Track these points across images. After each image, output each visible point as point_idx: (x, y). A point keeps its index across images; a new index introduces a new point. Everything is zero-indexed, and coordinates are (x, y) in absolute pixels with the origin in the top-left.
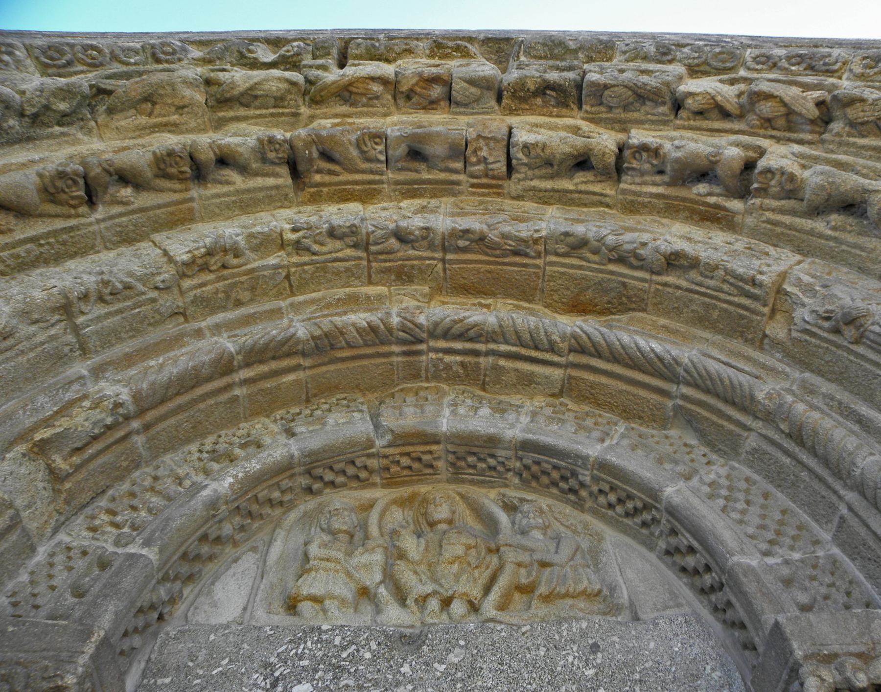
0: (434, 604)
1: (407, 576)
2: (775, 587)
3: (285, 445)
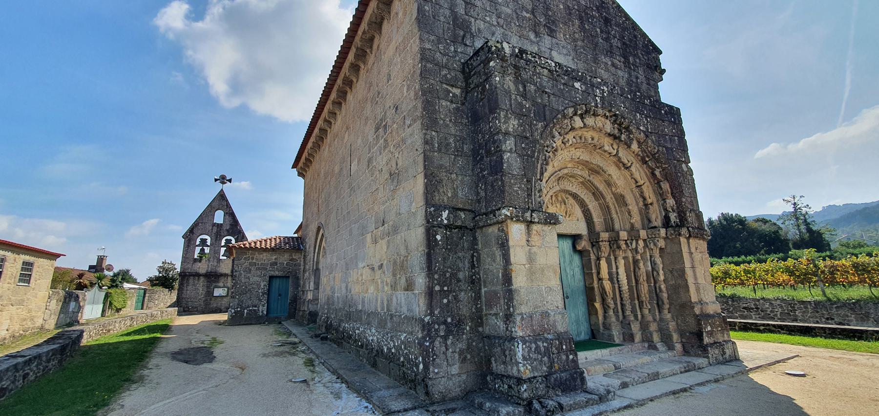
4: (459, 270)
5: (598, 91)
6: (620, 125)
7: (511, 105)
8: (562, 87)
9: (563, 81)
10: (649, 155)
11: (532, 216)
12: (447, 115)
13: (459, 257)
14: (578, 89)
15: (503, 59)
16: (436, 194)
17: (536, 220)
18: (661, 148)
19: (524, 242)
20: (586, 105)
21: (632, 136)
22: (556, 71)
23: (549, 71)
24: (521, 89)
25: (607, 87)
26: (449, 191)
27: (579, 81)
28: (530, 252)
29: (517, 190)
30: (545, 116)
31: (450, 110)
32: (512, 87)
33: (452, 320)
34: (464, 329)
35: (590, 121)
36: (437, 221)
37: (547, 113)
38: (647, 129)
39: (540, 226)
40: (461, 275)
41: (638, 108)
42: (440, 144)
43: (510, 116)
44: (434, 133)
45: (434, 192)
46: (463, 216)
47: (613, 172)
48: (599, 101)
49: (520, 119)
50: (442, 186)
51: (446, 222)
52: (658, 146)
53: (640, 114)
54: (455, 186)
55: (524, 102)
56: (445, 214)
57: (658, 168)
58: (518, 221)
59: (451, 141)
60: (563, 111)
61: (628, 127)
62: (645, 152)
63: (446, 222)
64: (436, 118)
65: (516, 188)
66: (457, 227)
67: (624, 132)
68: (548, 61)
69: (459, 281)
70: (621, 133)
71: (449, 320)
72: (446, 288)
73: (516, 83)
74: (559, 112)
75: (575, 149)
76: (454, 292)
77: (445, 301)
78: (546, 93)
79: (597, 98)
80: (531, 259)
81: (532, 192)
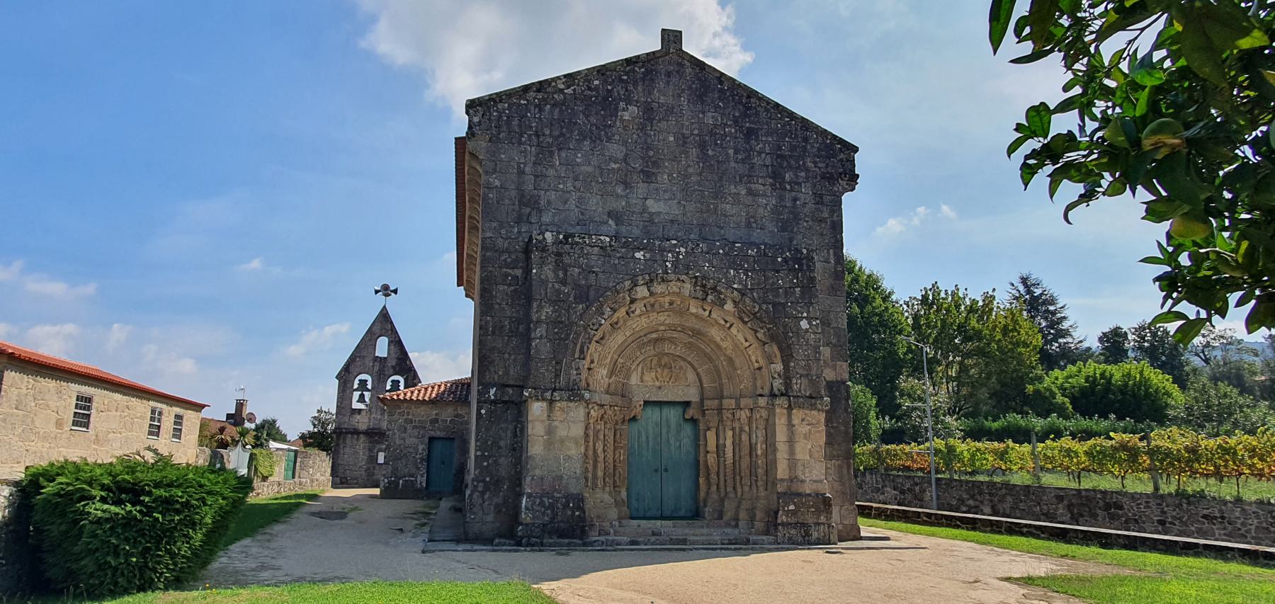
1: (659, 376)
4: (501, 439)
5: (670, 255)
6: (704, 286)
8: (616, 262)
9: (618, 255)
11: (552, 394)
12: (503, 298)
13: (502, 428)
14: (640, 259)
15: (544, 249)
16: (487, 373)
17: (558, 398)
18: (764, 307)
20: (649, 274)
21: (722, 296)
22: (611, 246)
23: (601, 248)
24: (561, 275)
25: (686, 248)
27: (642, 250)
28: (550, 425)
30: (588, 296)
32: (551, 275)
35: (659, 288)
37: (592, 293)
38: (746, 286)
39: (564, 403)
40: (502, 443)
41: (734, 262)
42: (494, 327)
43: (544, 304)
44: (489, 318)
46: (511, 392)
47: (715, 333)
48: (670, 266)
51: (493, 397)
52: (760, 305)
53: (735, 270)
55: (562, 288)
56: (492, 391)
57: (762, 328)
58: (538, 400)
59: (506, 323)
60: (615, 286)
61: (716, 287)
62: (744, 312)
63: (493, 397)
65: (544, 373)
66: (503, 402)
68: (602, 238)
69: (500, 448)
70: (708, 295)
71: (488, 479)
72: (486, 454)
73: (555, 271)
74: (607, 289)
76: (495, 456)
77: (485, 464)
78: (594, 272)
79: (667, 263)
80: (550, 431)
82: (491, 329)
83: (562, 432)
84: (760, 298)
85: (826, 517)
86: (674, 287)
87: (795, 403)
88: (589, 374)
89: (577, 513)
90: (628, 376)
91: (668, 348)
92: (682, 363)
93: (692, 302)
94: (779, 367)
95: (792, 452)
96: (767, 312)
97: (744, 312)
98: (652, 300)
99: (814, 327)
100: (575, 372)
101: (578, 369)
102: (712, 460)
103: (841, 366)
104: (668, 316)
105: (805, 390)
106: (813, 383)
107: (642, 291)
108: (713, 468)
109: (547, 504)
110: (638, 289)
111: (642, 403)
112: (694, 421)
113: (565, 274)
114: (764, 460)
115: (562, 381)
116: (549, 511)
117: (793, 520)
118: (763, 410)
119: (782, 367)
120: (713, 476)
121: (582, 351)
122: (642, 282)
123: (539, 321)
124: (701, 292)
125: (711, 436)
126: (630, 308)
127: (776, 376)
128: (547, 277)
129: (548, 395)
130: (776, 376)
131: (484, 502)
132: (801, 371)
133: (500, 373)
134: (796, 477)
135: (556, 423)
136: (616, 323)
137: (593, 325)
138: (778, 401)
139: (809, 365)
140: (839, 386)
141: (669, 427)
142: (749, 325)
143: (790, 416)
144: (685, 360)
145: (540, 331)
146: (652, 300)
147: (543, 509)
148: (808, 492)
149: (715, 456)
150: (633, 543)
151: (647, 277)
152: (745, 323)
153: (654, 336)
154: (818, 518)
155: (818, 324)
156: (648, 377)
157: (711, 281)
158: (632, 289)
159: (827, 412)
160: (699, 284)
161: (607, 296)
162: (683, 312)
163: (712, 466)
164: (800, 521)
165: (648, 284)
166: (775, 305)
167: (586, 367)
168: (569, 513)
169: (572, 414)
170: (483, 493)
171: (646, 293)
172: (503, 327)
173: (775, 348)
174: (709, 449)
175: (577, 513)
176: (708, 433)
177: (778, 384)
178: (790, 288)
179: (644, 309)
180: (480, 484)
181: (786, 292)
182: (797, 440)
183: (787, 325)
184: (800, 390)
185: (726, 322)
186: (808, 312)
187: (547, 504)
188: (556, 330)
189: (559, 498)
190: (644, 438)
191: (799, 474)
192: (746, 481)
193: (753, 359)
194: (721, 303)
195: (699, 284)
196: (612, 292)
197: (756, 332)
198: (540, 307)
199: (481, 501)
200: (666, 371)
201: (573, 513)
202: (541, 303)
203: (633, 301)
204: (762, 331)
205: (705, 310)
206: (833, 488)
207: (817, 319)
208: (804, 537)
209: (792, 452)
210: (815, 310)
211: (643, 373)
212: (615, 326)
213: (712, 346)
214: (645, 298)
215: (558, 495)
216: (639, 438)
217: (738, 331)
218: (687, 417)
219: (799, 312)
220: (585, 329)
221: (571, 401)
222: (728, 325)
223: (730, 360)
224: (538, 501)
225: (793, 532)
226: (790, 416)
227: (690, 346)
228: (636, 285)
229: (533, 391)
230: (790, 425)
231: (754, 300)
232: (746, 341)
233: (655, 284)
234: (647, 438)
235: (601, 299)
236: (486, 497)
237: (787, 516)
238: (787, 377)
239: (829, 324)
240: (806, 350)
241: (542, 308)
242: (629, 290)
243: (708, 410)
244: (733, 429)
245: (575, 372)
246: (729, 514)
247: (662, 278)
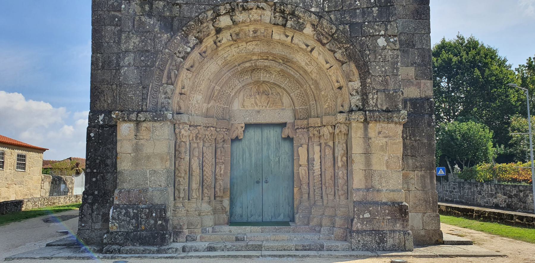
0: (261, 107)
1: (257, 102)
2: (299, 112)
3: (239, 85)
4: (108, 158)
6: (283, 12)
7: (134, 26)
10: (327, 36)
11: (137, 116)
13: (108, 148)
16: (98, 102)
18: (341, 27)
19: (132, 136)
20: (230, 4)
21: (301, 21)
24: (147, 8)
26: (109, 98)
28: (137, 144)
29: (132, 96)
31: (114, 33)
32: (138, 9)
33: (99, 193)
34: (108, 200)
35: (240, 17)
36: (94, 122)
37: (176, 23)
38: (323, 9)
39: (149, 124)
42: (103, 63)
43: (131, 35)
44: (99, 55)
45: (96, 101)
47: (300, 59)
49: (142, 36)
50: (103, 96)
51: (101, 123)
54: (114, 94)
56: (101, 117)
57: (340, 48)
59: (114, 58)
60: (198, 16)
62: (322, 35)
63: (101, 123)
64: (102, 43)
67: (290, 18)
69: (107, 165)
70: (287, 21)
71: (96, 193)
72: (95, 171)
73: (142, 6)
74: (190, 19)
75: (247, 43)
77: (94, 179)
78: (177, 4)
80: (137, 149)
81: (147, 96)
82: (100, 64)
83: (148, 149)
84: (337, 19)
85: (403, 224)
86: (255, 15)
87: (371, 117)
88: (180, 98)
89: (160, 222)
90: (231, 103)
91: (263, 76)
92: (279, 90)
93: (275, 29)
94: (357, 84)
95: (368, 163)
96: (343, 32)
97: (322, 35)
98: (237, 29)
99: (391, 44)
100: (163, 96)
101: (166, 93)
102: (303, 172)
103: (425, 84)
104: (256, 45)
105: (381, 105)
106: (390, 97)
107: (225, 21)
108: (305, 181)
109: (132, 214)
110: (221, 18)
111: (243, 125)
112: (289, 139)
113: (151, 8)
114: (345, 172)
115: (149, 104)
116: (134, 221)
117: (368, 227)
118: (343, 125)
119: (360, 84)
120: (305, 186)
121: (169, 77)
122: (224, 12)
123: (127, 51)
124: (281, 19)
125: (302, 152)
126: (217, 38)
127: (354, 93)
128: (134, 11)
129: (133, 116)
130: (354, 93)
131: (93, 212)
132: (378, 87)
133: (109, 102)
134: (372, 187)
135: (142, 142)
136: (205, 52)
137: (180, 53)
138: (354, 116)
139: (386, 81)
140: (423, 102)
141: (269, 144)
142: (327, 46)
143: (366, 129)
144: (280, 86)
145: (129, 59)
146: (237, 29)
147: (128, 219)
148: (384, 201)
149: (306, 169)
150: (211, 249)
151: (228, 6)
152: (324, 45)
153: (248, 65)
154: (394, 225)
155: (396, 41)
156: (249, 102)
157: (289, 6)
158: (215, 18)
159: (405, 126)
160: (278, 10)
161: (190, 26)
162: (268, 40)
163: (303, 177)
164: (376, 228)
165: (231, 12)
166: (351, 25)
167: (177, 91)
168: (152, 222)
169: (157, 133)
170: (92, 204)
171: (231, 23)
172: (110, 62)
173: (353, 66)
174: (301, 163)
175: (160, 222)
176: (300, 148)
177: (356, 100)
178: (368, 8)
179: (230, 38)
180: (90, 197)
181: (363, 13)
182: (373, 152)
183: (364, 43)
184: (376, 105)
185: (307, 46)
186: (386, 30)
187: (132, 214)
188: (143, 58)
189: (143, 209)
190: (247, 155)
191: (376, 184)
192: (330, 191)
193: (334, 78)
194: (300, 28)
195: (278, 10)
196: (195, 22)
197: (334, 52)
198: (128, 38)
199: (90, 211)
200: (264, 97)
201: (156, 222)
202: (129, 34)
203: (218, 31)
204: (340, 51)
205: (287, 36)
206: (416, 197)
207: (395, 36)
208: (379, 244)
209: (368, 163)
210: (393, 28)
211: (244, 100)
212: (203, 54)
213: (301, 72)
214: (229, 28)
215: (143, 206)
216: (243, 155)
217: (319, 54)
218: (283, 136)
219: (376, 31)
220: (171, 56)
221: (155, 121)
222: (309, 49)
223: (316, 84)
224: (124, 211)
225: (368, 239)
226: (366, 129)
227: (283, 74)
228: (219, 15)
229: (120, 113)
230: (367, 138)
231: (331, 21)
232: (327, 63)
233: (237, 13)
234: (250, 155)
235: (184, 29)
236: (95, 207)
237: (362, 224)
238: (364, 95)
239: (414, 45)
240: (383, 67)
241: (130, 39)
242: (212, 20)
243: (298, 128)
244: (320, 145)
245: (163, 96)
246: (315, 220)
247: (242, 6)
